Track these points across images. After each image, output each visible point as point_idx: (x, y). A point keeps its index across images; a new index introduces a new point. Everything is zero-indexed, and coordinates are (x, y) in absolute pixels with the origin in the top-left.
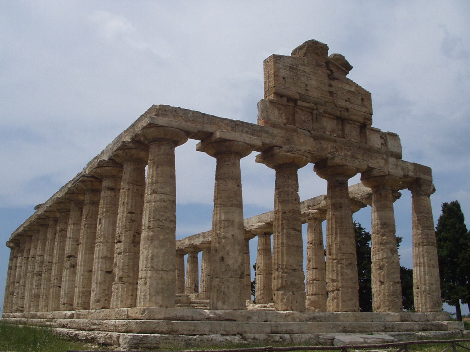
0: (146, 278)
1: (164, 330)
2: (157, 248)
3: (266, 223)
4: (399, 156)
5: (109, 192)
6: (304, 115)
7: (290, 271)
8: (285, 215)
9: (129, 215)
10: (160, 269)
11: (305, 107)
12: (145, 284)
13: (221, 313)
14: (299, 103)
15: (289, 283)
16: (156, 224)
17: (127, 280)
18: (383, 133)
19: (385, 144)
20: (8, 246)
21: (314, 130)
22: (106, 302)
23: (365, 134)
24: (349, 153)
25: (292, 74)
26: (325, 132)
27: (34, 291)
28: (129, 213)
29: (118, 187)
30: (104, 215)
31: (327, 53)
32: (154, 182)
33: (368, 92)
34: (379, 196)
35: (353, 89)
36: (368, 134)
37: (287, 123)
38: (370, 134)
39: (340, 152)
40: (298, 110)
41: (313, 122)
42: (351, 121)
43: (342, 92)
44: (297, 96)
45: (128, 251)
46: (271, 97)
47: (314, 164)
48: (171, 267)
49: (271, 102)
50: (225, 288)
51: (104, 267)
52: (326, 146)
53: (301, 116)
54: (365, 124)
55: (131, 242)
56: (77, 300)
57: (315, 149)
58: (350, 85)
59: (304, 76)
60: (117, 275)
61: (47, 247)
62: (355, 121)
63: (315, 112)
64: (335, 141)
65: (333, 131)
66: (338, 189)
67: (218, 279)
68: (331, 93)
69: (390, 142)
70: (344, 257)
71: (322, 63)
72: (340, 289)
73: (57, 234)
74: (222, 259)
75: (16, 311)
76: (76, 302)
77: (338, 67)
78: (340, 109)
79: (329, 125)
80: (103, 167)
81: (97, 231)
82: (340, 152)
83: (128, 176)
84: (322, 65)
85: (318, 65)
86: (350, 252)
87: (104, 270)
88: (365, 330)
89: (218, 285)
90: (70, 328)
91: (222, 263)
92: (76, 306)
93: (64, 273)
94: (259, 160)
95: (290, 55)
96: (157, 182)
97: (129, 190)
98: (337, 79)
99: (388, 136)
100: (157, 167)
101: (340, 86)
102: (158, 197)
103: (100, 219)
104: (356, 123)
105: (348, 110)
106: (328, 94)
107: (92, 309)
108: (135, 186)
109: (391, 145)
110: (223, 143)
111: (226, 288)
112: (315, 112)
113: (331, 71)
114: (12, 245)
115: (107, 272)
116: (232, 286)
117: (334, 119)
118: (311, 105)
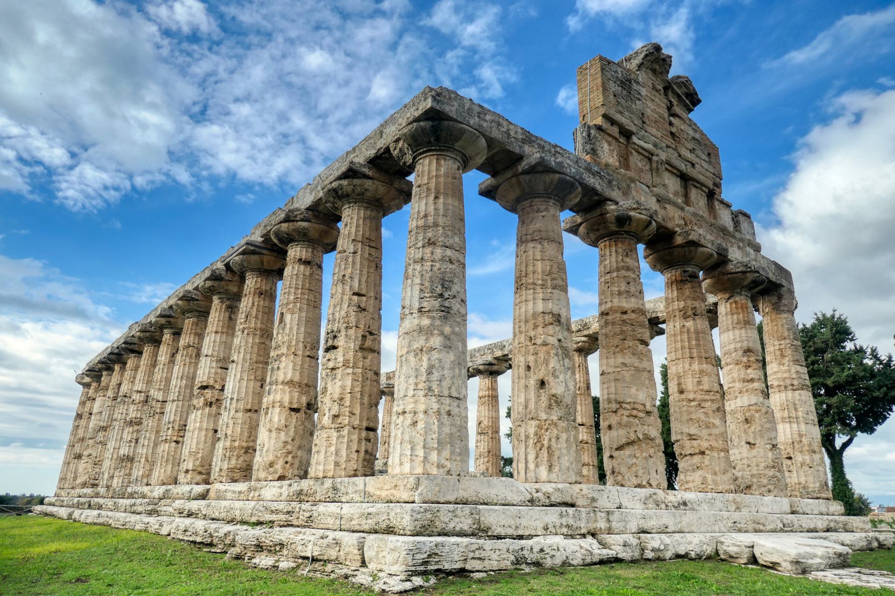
0: (415, 413)
1: (466, 528)
2: (440, 351)
3: (495, 358)
5: (302, 267)
7: (642, 415)
9: (355, 298)
10: (446, 393)
11: (643, 148)
12: (415, 423)
13: (550, 490)
14: (635, 139)
15: (641, 436)
16: (436, 304)
17: (349, 422)
20: (79, 383)
22: (288, 465)
27: (124, 451)
28: (354, 294)
29: (317, 261)
30: (291, 306)
31: (668, 72)
32: (431, 225)
34: (734, 305)
35: (697, 136)
44: (633, 129)
45: (351, 365)
46: (599, 121)
49: (599, 128)
50: (550, 440)
51: (287, 399)
55: (357, 348)
56: (219, 463)
59: (639, 99)
60: (327, 411)
61: (158, 375)
62: (702, 185)
64: (682, 209)
65: (676, 194)
66: (689, 285)
69: (744, 225)
70: (707, 397)
72: (707, 452)
73: (180, 352)
74: (542, 383)
75: (84, 485)
76: (218, 469)
77: (678, 96)
79: (673, 184)
80: (294, 221)
81: (275, 336)
87: (286, 404)
88: (761, 527)
91: (541, 391)
92: (217, 474)
93: (192, 417)
96: (438, 226)
97: (355, 253)
100: (436, 198)
102: (439, 252)
103: (282, 314)
104: (704, 188)
105: (693, 165)
107: (259, 480)
108: (367, 248)
111: (553, 440)
112: (655, 158)
113: (671, 102)
114: (87, 380)
115: (292, 410)
116: (564, 436)
117: (677, 176)
118: (649, 146)
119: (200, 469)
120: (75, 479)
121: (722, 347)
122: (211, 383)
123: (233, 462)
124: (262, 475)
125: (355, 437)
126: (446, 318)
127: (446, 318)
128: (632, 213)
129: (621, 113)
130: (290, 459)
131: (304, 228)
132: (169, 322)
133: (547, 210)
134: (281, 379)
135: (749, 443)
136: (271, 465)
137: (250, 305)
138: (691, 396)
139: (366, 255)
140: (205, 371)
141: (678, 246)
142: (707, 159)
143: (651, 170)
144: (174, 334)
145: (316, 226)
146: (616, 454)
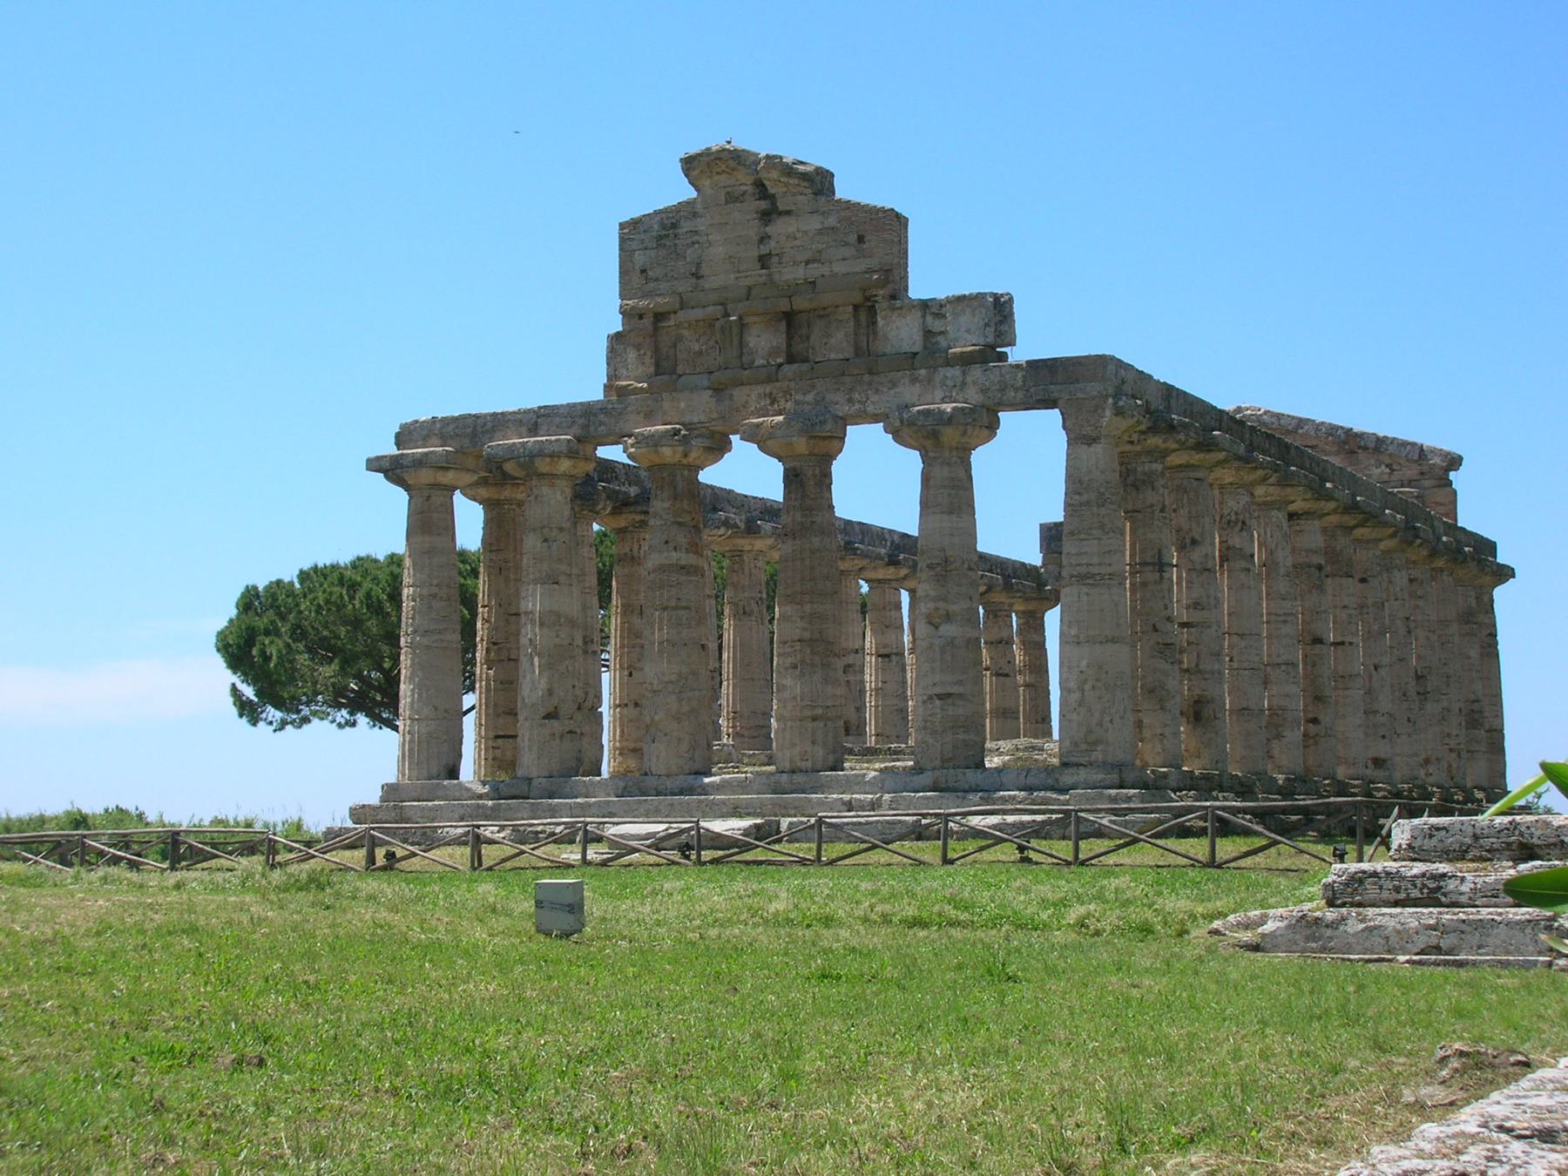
23: (874, 323)
24: (810, 398)
35: (832, 221)
36: (881, 322)
39: (782, 402)
40: (685, 332)
43: (797, 243)
48: (426, 711)
57: (715, 415)
64: (770, 379)
65: (773, 352)
71: (744, 188)
82: (782, 402)
84: (744, 194)
85: (732, 198)
86: (796, 637)
98: (788, 213)
101: (792, 229)
106: (758, 265)
142: (849, 252)
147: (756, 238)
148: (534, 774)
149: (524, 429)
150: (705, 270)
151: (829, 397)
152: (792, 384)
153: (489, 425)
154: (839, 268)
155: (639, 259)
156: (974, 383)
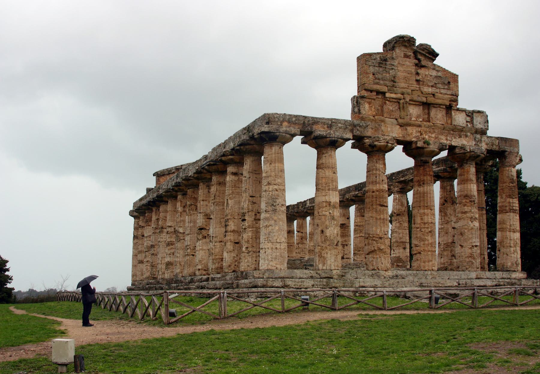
1: (279, 285)
4: (483, 132)
5: (233, 177)
6: (392, 106)
8: (374, 194)
10: (275, 241)
11: (393, 98)
14: (387, 95)
18: (469, 112)
19: (472, 122)
21: (401, 118)
23: (451, 114)
24: (433, 135)
25: (381, 69)
26: (411, 119)
29: (240, 172)
33: (455, 75)
35: (440, 74)
36: (453, 114)
37: (377, 115)
38: (455, 115)
40: (387, 102)
41: (400, 111)
42: (437, 104)
43: (429, 79)
44: (385, 89)
47: (402, 146)
52: (411, 131)
53: (390, 107)
54: (450, 107)
57: (401, 136)
58: (437, 70)
63: (401, 101)
64: (420, 126)
65: (418, 117)
67: (320, 247)
68: (417, 81)
78: (426, 96)
82: (424, 135)
83: (248, 167)
89: (319, 252)
90: (208, 288)
94: (354, 146)
95: (381, 50)
99: (474, 114)
101: (427, 73)
104: (442, 106)
105: (434, 95)
106: (415, 83)
109: (478, 122)
110: (321, 138)
112: (401, 101)
118: (399, 96)
119: (205, 268)
120: (142, 275)
121: (458, 192)
122: (204, 226)
123: (217, 265)
124: (227, 271)
125: (254, 255)
126: (275, 213)
127: (275, 213)
128: (376, 143)
129: (377, 84)
130: (236, 264)
131: (232, 159)
132: (180, 189)
133: (327, 153)
134: (229, 230)
135: (461, 245)
136: (230, 266)
137: (215, 190)
138: (418, 226)
139: (254, 179)
140: (200, 221)
141: (414, 149)
143: (399, 108)
144: (183, 195)
145: (237, 157)
146: (367, 256)
147: (414, 73)
148: (333, 268)
149: (326, 126)
150: (397, 80)
151: (440, 137)
152: (428, 129)
153: (311, 122)
154: (442, 91)
155: (372, 69)
156: (484, 141)
